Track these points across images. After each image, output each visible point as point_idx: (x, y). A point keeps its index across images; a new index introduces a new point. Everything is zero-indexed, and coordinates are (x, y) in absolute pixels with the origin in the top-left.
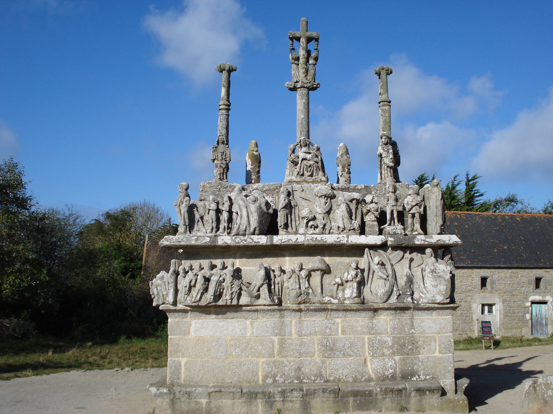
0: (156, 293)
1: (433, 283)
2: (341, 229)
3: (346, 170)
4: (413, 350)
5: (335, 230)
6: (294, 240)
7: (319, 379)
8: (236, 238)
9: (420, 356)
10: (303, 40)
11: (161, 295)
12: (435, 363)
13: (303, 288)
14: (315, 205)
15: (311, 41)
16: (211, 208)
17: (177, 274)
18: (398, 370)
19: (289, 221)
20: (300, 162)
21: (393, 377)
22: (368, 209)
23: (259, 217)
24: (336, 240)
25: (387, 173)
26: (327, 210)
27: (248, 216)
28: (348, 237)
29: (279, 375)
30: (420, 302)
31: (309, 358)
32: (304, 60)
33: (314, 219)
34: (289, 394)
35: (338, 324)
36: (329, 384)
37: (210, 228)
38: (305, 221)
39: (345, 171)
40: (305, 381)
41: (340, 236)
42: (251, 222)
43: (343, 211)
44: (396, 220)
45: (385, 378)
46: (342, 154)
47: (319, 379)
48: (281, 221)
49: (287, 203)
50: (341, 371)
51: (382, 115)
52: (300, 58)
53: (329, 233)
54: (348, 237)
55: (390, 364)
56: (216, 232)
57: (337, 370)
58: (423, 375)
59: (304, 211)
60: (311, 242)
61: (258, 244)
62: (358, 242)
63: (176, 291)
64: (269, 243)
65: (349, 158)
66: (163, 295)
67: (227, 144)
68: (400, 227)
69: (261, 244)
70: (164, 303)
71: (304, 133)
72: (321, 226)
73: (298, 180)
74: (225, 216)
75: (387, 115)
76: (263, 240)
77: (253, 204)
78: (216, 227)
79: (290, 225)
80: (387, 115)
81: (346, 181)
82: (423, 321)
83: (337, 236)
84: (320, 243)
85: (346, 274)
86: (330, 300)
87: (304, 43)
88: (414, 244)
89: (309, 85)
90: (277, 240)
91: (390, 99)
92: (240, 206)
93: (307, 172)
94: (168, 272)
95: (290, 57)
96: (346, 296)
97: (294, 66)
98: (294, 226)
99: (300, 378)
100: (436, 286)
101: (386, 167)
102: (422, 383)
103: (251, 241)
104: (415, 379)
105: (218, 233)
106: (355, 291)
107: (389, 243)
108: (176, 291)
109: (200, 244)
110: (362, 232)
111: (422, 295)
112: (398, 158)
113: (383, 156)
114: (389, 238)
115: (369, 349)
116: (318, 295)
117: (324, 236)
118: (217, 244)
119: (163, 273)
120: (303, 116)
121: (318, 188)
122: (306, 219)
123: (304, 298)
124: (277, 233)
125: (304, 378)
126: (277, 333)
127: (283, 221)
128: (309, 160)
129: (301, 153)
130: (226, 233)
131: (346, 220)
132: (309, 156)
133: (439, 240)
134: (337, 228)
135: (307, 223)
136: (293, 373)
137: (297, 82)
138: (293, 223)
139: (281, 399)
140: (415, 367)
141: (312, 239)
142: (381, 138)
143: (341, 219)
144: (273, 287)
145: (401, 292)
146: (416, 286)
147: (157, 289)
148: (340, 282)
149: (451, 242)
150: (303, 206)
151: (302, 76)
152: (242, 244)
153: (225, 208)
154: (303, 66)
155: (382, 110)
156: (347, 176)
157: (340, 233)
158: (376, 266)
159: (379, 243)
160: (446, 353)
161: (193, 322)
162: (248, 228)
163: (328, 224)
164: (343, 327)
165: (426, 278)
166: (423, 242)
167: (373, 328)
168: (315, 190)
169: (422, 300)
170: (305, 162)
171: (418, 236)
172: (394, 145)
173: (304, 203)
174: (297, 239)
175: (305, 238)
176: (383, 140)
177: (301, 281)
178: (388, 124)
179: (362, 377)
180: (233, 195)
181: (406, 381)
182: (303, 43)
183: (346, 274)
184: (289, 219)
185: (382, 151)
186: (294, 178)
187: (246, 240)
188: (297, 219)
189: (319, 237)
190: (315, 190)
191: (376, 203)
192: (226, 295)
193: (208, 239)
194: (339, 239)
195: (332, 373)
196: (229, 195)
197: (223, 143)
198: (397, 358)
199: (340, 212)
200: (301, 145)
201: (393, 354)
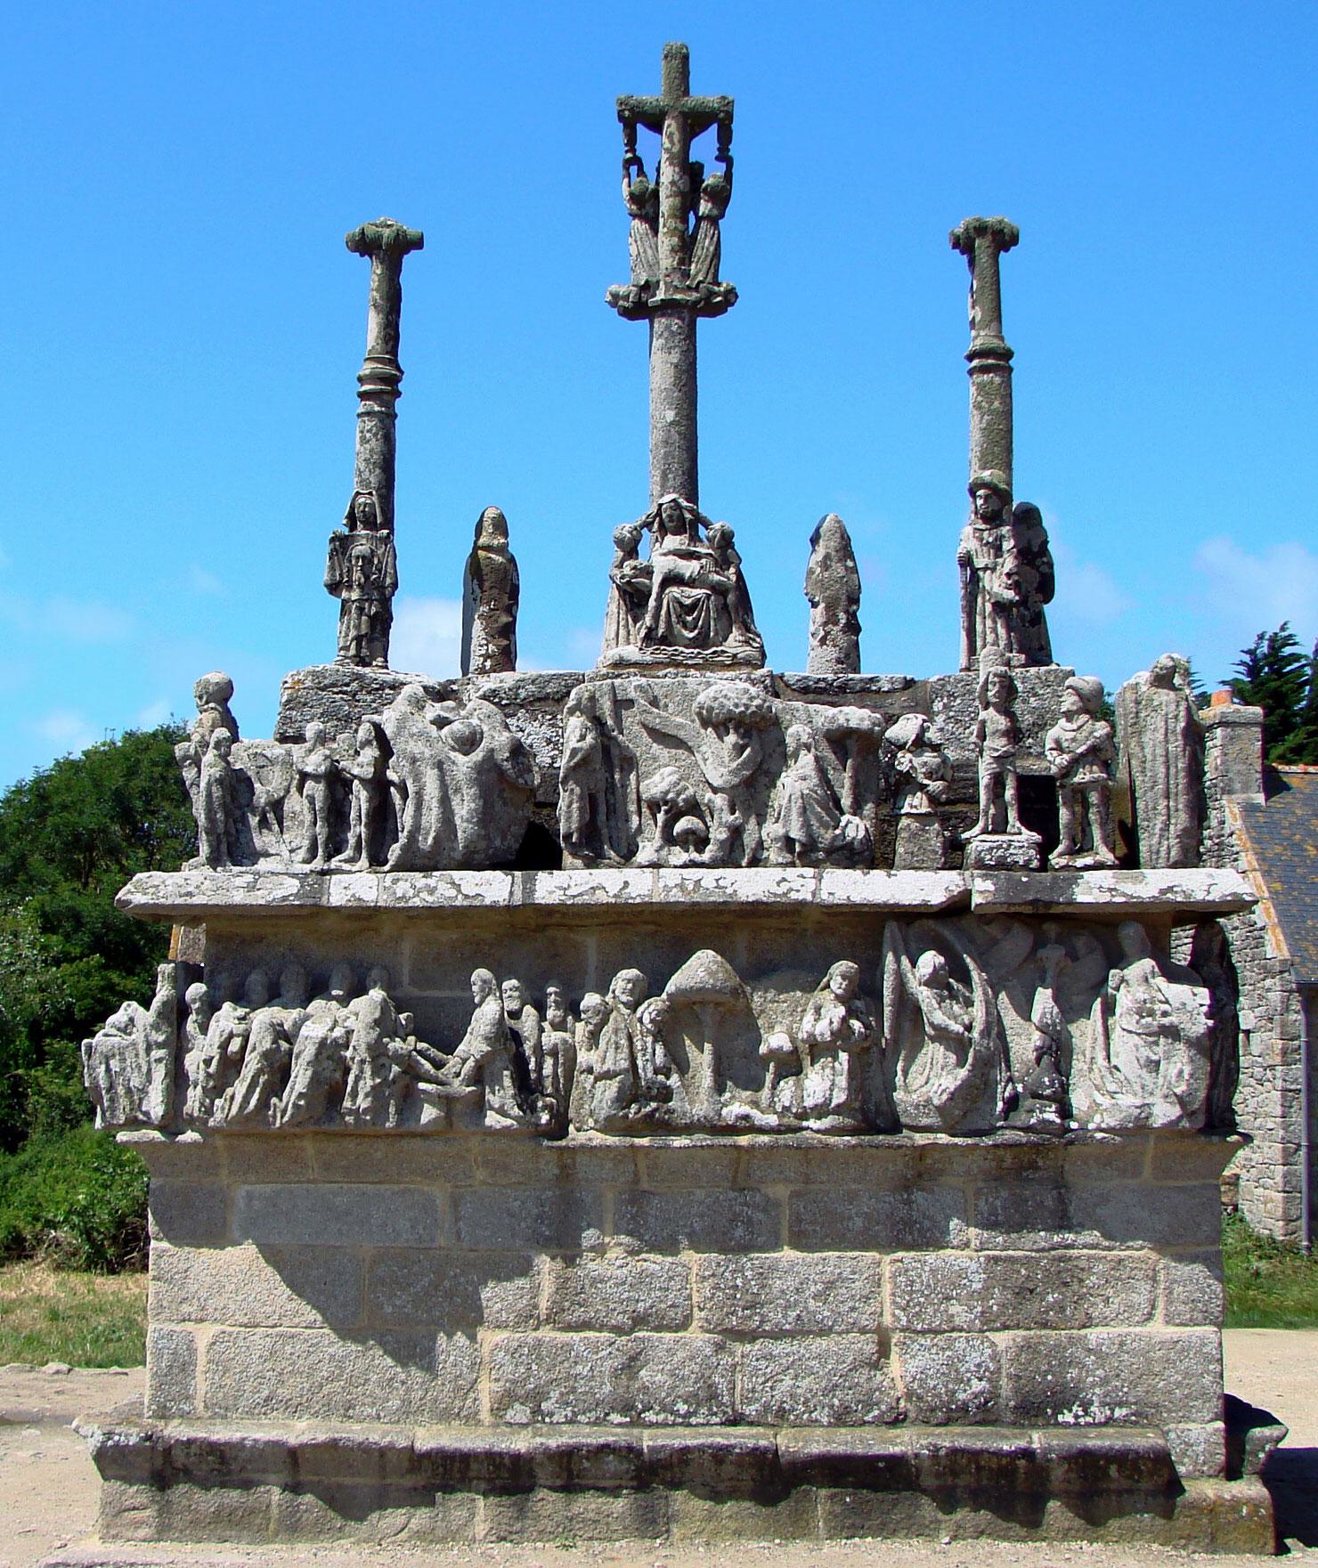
0: (103, 1083)
1: (1145, 1052)
3: (843, 618)
4: (1063, 1309)
5: (773, 854)
7: (704, 1410)
8: (395, 881)
9: (1094, 1335)
10: (670, 125)
11: (121, 1090)
12: (1149, 1361)
13: (646, 1072)
15: (705, 128)
16: (309, 769)
17: (177, 1012)
18: (1004, 1381)
19: (602, 817)
20: (655, 590)
21: (985, 1413)
22: (904, 768)
25: (994, 630)
27: (445, 801)
29: (555, 1395)
30: (1091, 1126)
31: (668, 1335)
32: (677, 201)
34: (586, 1464)
35: (777, 1204)
36: (740, 1430)
37: (306, 843)
38: (661, 817)
39: (836, 624)
40: (650, 1416)
41: (791, 873)
44: (1012, 815)
45: (955, 1414)
46: (827, 557)
47: (704, 1410)
48: (569, 819)
50: (788, 1381)
51: (978, 407)
52: (662, 195)
53: (755, 862)
55: (974, 1358)
56: (328, 858)
57: (773, 1379)
58: (1103, 1404)
59: (657, 778)
60: (676, 896)
61: (476, 903)
62: (857, 898)
63: (178, 1080)
64: (518, 899)
65: (855, 570)
66: (129, 1091)
67: (389, 522)
68: (1030, 836)
69: (487, 902)
70: (133, 1124)
71: (675, 480)
72: (718, 834)
73: (648, 658)
74: (360, 799)
75: (996, 404)
76: (494, 887)
78: (329, 839)
79: (605, 831)
80: (996, 404)
81: (839, 661)
82: (1104, 1199)
83: (778, 873)
85: (809, 1017)
86: (746, 1117)
87: (676, 138)
88: (1072, 903)
89: (695, 295)
90: (550, 887)
91: (1009, 343)
92: (414, 761)
93: (685, 627)
94: (147, 1007)
95: (625, 192)
96: (809, 1103)
97: (639, 226)
99: (633, 1407)
100: (1153, 1066)
101: (989, 607)
102: (1093, 1432)
103: (453, 892)
104: (1067, 1417)
105: (334, 863)
106: (842, 1081)
107: (977, 899)
108: (178, 1080)
110: (874, 855)
111: (1099, 1099)
112: (1044, 569)
113: (979, 562)
114: (978, 881)
115: (894, 1302)
116: (703, 1097)
117: (729, 874)
118: (324, 901)
119: (129, 1009)
120: (670, 415)
121: (711, 692)
123: (648, 1109)
124: (554, 864)
125: (648, 1408)
126: (548, 1239)
127: (575, 815)
128: (691, 583)
129: (660, 556)
130: (364, 862)
132: (689, 568)
133: (1170, 889)
136: (607, 1388)
137: (648, 287)
139: (559, 1482)
140: (1073, 1373)
141: (681, 886)
142: (973, 493)
144: (532, 1066)
145: (1020, 1088)
146: (1078, 1065)
147: (108, 1070)
148: (787, 1046)
149: (1215, 896)
150: (655, 759)
151: (667, 261)
152: (417, 902)
153: (361, 765)
154: (672, 223)
155: (981, 388)
156: (842, 640)
157: (793, 864)
158: (923, 988)
159: (937, 898)
160: (1193, 1322)
161: (241, 1192)
163: (752, 824)
164: (797, 1219)
165: (1116, 1035)
166: (1105, 898)
167: (909, 1223)
168: (701, 698)
169: (1097, 1118)
170: (674, 591)
171: (1086, 874)
172: (1029, 518)
174: (626, 884)
175: (656, 881)
176: (980, 502)
177: (639, 1045)
178: (1000, 444)
179: (869, 1406)
180: (389, 719)
181: (1034, 1426)
182: (670, 137)
183: (809, 1017)
184: (602, 809)
185: (972, 545)
186: (632, 652)
187: (432, 891)
191: (936, 748)
192: (354, 1095)
193: (292, 886)
194: (784, 887)
195: (753, 1390)
196: (376, 718)
197: (370, 523)
198: (1003, 1339)
199: (796, 780)
200: (662, 524)
201: (989, 1323)
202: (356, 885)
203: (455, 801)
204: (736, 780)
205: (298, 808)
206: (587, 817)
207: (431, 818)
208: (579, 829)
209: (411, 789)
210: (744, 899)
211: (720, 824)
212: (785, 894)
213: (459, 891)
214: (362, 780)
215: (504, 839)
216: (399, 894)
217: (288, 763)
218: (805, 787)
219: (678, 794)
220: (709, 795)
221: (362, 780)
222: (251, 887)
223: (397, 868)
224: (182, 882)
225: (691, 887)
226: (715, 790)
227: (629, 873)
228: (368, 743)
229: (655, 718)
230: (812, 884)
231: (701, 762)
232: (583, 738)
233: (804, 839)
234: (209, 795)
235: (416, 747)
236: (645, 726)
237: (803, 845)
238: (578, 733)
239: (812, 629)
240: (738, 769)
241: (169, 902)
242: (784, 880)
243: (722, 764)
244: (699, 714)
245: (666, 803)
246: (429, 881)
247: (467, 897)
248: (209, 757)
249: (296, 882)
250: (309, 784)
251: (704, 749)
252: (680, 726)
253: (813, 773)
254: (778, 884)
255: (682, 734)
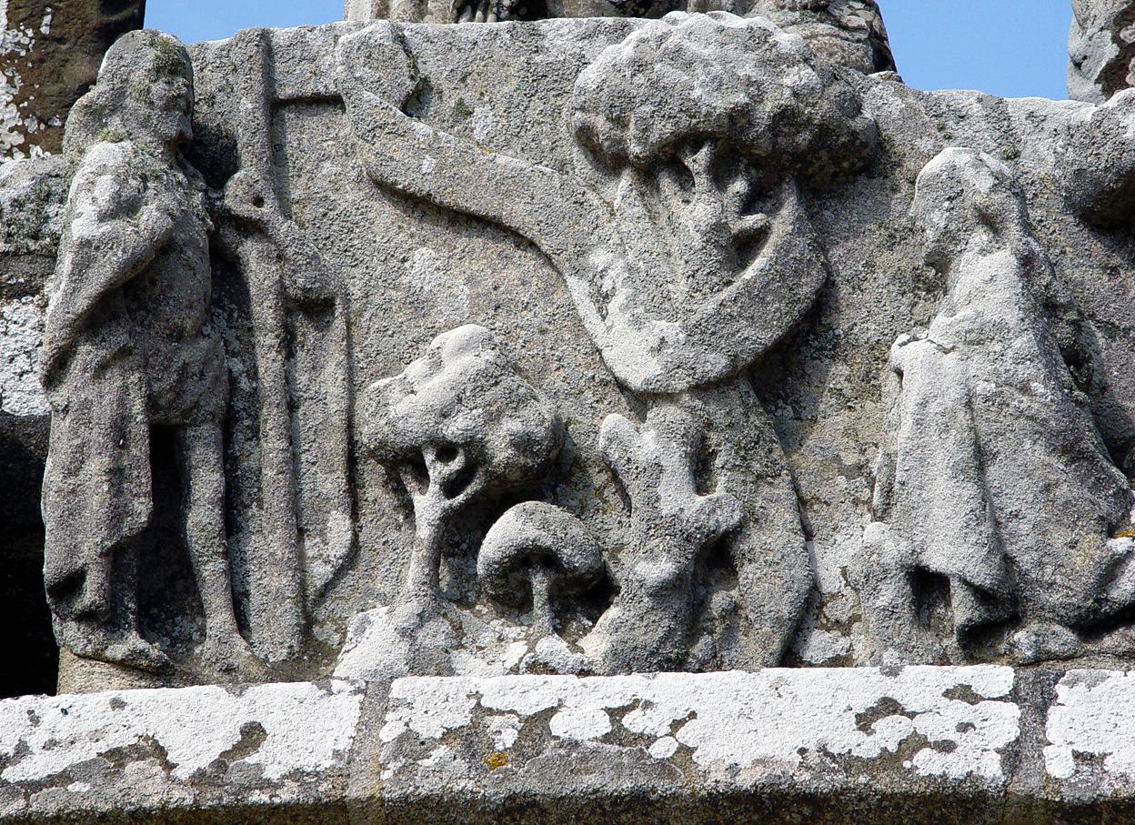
2: (961, 610)
6: (192, 754)
14: (578, 288)
19: (202, 517)
24: (846, 739)
26: (758, 335)
28: (1035, 700)
33: (554, 470)
38: (429, 504)
43: (976, 338)
48: (71, 514)
49: (165, 248)
54: (1035, 700)
79: (211, 570)
84: (590, 781)
98: (270, 583)
122: (438, 471)
127: (96, 500)
131: (1026, 468)
134: (891, 593)
135: (460, 533)
138: (267, 541)
141: (469, 739)
143: (946, 452)
150: (419, 305)
163: (773, 539)
168: (590, 77)
173: (427, 260)
174: (252, 735)
184: (206, 483)
188: (330, 483)
189: (582, 712)
190: (590, 77)
194: (889, 732)
204: (716, 364)
206: (142, 508)
208: (114, 556)
210: (718, 778)
211: (654, 525)
212: (889, 760)
218: (980, 372)
219: (494, 418)
220: (614, 421)
225: (508, 738)
226: (641, 401)
227: (275, 702)
229: (419, 155)
230: (1004, 722)
231: (587, 310)
232: (125, 207)
233: (983, 574)
236: (387, 189)
237: (982, 595)
238: (105, 189)
239: (1076, 44)
240: (722, 316)
242: (889, 706)
243: (661, 306)
244: (585, 137)
245: (446, 451)
251: (599, 258)
252: (509, 184)
253: (1012, 317)
254: (864, 722)
255: (517, 213)
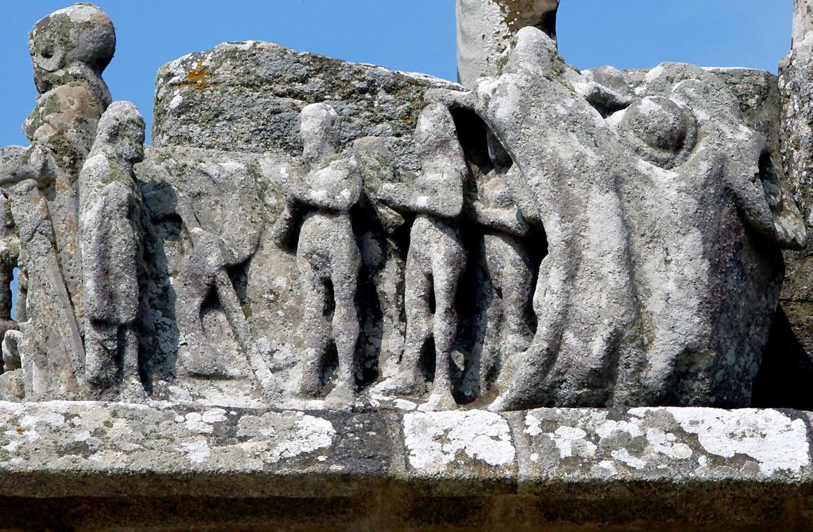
8: (549, 425)
16: (317, 195)
23: (715, 268)
27: (629, 260)
37: (311, 354)
42: (654, 305)
69: (767, 471)
77: (666, 164)
92: (559, 175)
103: (683, 451)
109: (256, 465)
118: (397, 469)
152: (607, 469)
162: (629, 353)
187: (637, 446)
202: (444, 437)
203: (651, 267)
205: (281, 282)
207: (599, 301)
209: (554, 232)
213: (698, 449)
214: (436, 218)
215: (739, 353)
216: (566, 452)
217: (258, 188)
221: (436, 218)
222: (225, 433)
223: (522, 404)
224: (59, 421)
228: (443, 144)
234: (104, 239)
235: (564, 147)
241: (35, 465)
246: (624, 426)
247: (716, 460)
248: (96, 161)
249: (326, 425)
250: (313, 226)
